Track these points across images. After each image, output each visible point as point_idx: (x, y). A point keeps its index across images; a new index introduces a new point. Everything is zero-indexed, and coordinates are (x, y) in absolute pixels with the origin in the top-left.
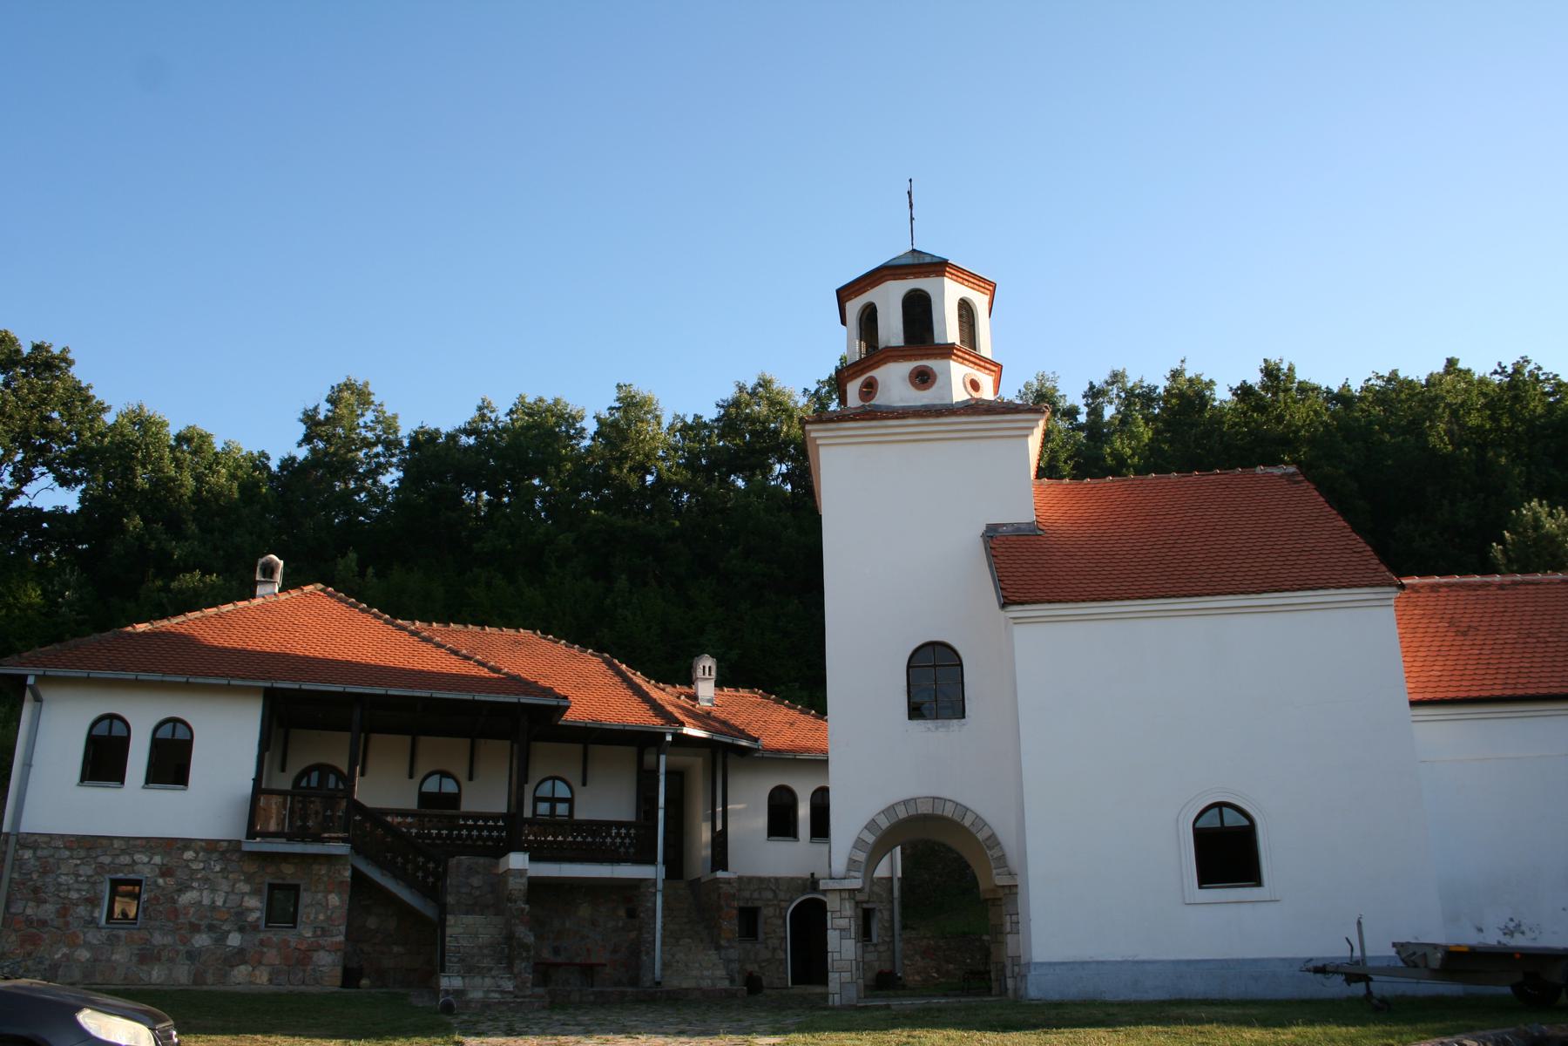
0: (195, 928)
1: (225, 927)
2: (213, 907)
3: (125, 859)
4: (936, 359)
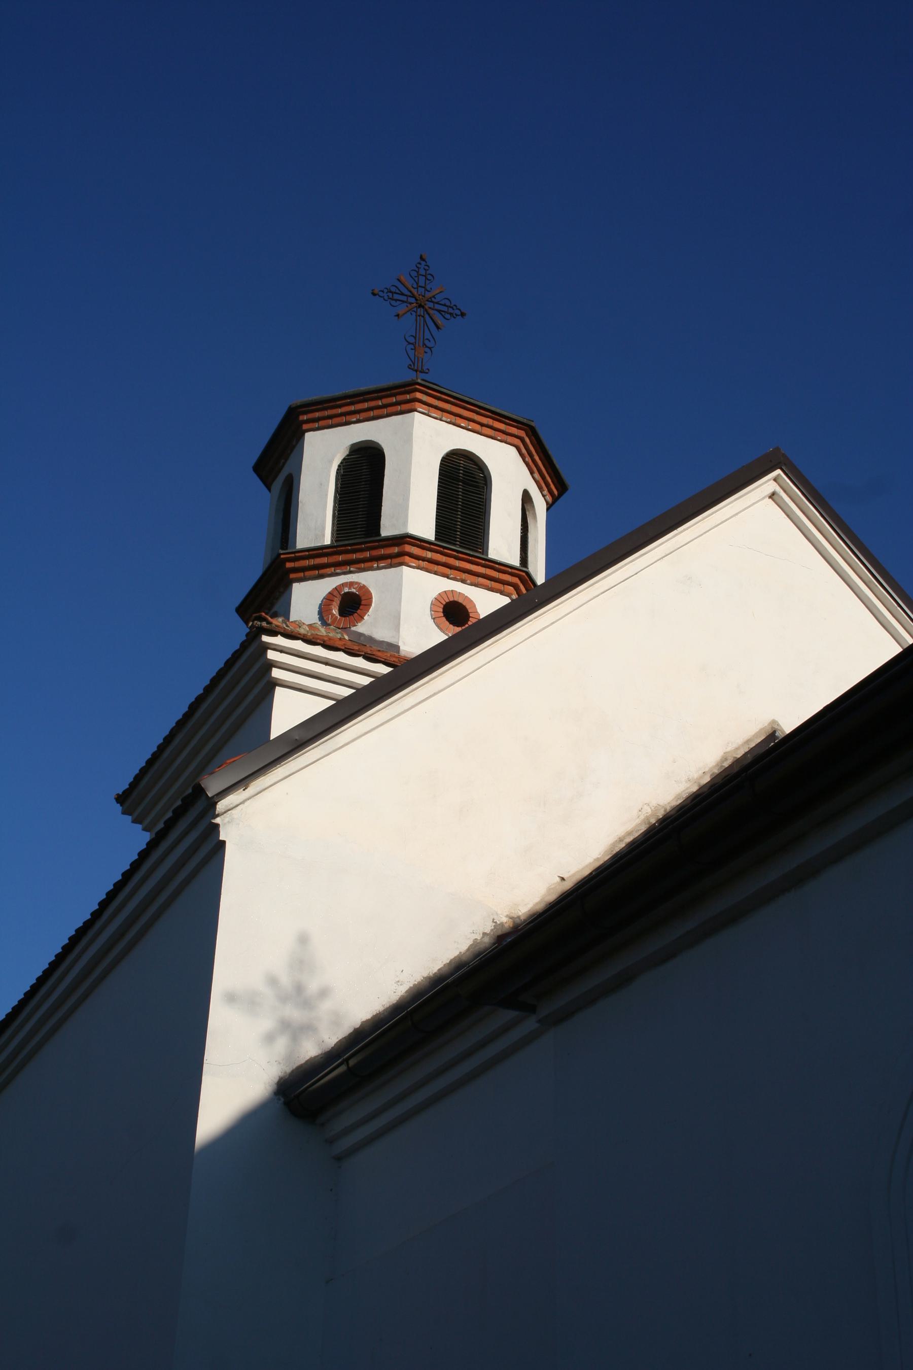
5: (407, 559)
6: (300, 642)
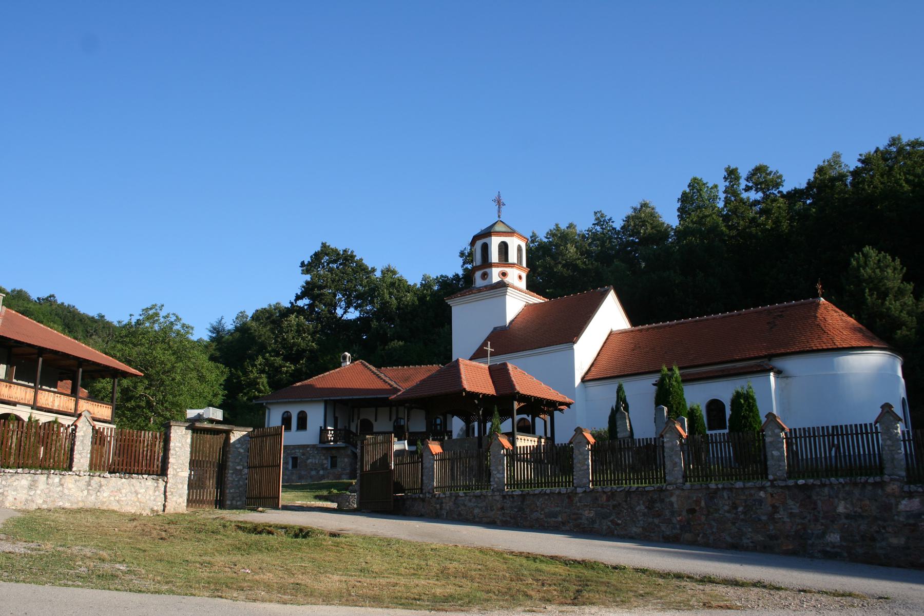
0: (312, 470)
1: (319, 469)
2: (316, 464)
3: (293, 451)
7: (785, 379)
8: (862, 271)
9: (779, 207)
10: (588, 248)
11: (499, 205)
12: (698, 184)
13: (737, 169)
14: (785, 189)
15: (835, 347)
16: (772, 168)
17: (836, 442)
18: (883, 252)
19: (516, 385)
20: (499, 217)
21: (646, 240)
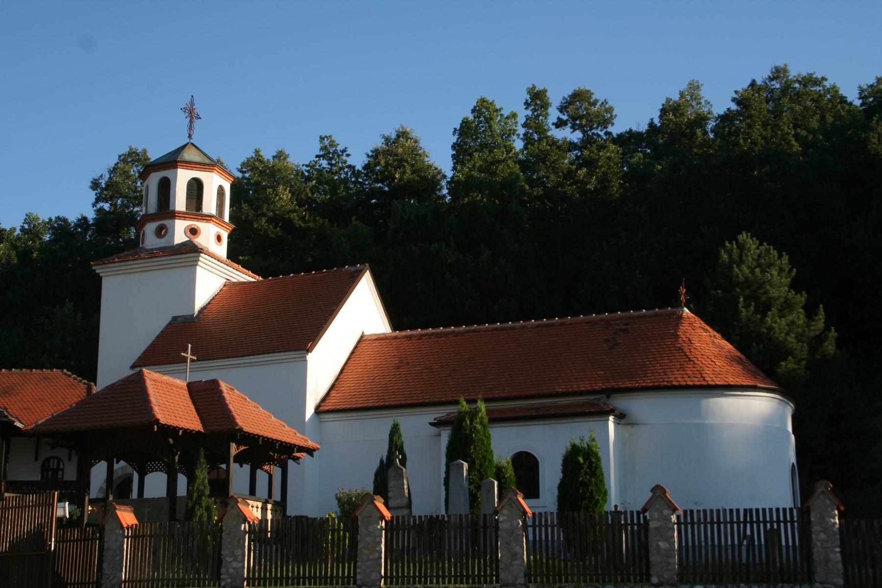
4: (168, 219)
5: (212, 221)
6: (213, 259)
7: (629, 427)
8: (736, 270)
9: (609, 158)
10: (310, 195)
11: (192, 118)
12: (487, 109)
13: (545, 91)
14: (616, 129)
15: (705, 383)
16: (598, 95)
17: (748, 532)
18: (765, 244)
19: (237, 417)
20: (190, 136)
21: (400, 191)
